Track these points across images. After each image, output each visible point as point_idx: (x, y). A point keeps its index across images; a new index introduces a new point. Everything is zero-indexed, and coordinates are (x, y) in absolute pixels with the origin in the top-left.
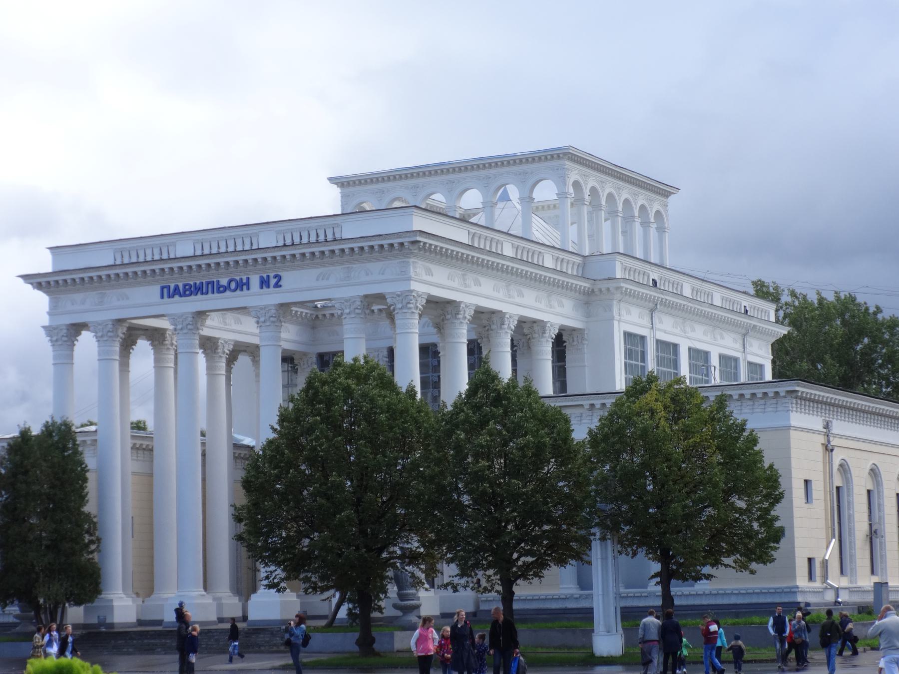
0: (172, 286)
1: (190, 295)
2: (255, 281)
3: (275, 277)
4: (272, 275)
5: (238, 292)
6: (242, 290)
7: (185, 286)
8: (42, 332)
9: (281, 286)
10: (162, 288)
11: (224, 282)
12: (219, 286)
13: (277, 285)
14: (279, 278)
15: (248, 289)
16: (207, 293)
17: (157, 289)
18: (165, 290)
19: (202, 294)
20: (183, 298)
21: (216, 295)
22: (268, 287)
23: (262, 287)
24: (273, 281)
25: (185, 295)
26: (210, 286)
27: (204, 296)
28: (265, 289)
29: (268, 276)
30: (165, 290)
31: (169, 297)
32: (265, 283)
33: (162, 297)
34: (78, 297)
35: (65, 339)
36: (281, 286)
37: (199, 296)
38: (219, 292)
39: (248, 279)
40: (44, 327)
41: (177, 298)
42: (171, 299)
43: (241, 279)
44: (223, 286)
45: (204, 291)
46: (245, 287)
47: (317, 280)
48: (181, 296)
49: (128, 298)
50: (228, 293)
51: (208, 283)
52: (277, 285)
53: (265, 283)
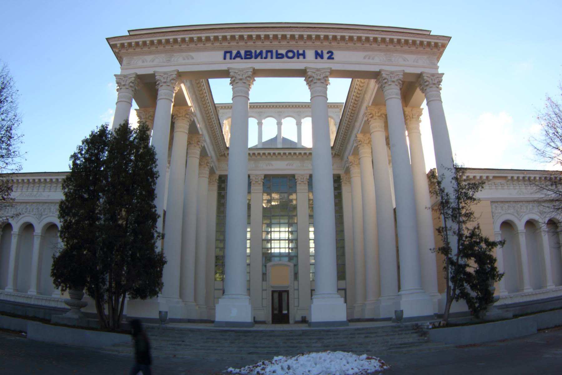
0: (234, 53)
1: (251, 58)
2: (310, 54)
3: (328, 53)
4: (325, 52)
5: (295, 59)
6: (298, 58)
7: (246, 52)
8: (114, 79)
9: (333, 59)
10: (226, 53)
11: (283, 52)
13: (330, 58)
15: (304, 58)
16: (266, 58)
17: (222, 53)
18: (228, 55)
19: (262, 58)
21: (274, 59)
23: (316, 58)
24: (326, 56)
25: (246, 58)
26: (269, 54)
27: (264, 60)
28: (319, 59)
29: (322, 52)
30: (228, 55)
31: (231, 59)
32: (319, 55)
33: (225, 58)
34: (149, 58)
35: (131, 84)
36: (333, 59)
37: (259, 59)
38: (277, 58)
39: (304, 51)
40: (115, 75)
41: (238, 59)
42: (232, 60)
43: (298, 51)
45: (264, 55)
46: (301, 57)
47: (365, 58)
48: (242, 59)
49: (193, 58)
50: (285, 59)
51: (267, 52)
52: (330, 58)
53: (319, 55)
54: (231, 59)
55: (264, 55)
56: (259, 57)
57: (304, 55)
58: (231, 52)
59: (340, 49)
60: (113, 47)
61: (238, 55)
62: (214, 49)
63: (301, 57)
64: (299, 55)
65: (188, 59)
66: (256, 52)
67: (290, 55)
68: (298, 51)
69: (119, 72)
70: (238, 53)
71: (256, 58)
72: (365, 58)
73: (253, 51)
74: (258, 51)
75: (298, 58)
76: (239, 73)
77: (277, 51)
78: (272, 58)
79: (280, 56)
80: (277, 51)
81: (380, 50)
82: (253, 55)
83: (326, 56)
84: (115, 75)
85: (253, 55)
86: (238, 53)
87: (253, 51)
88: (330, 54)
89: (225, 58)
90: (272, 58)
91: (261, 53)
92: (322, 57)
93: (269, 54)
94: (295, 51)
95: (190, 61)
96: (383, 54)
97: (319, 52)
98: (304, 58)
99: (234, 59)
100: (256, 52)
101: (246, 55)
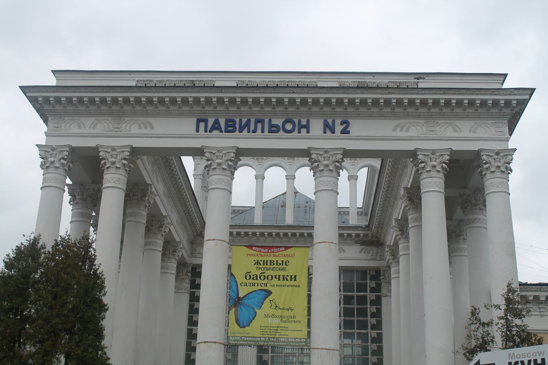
3: (341, 124)
6: (299, 132)
7: (227, 121)
8: (37, 151)
9: (348, 133)
10: (199, 121)
11: (278, 122)
12: (271, 126)
13: (345, 131)
14: (346, 123)
15: (308, 132)
16: (254, 131)
17: (194, 121)
18: (202, 125)
19: (249, 132)
20: (224, 133)
22: (333, 132)
23: (325, 133)
24: (339, 128)
26: (259, 126)
27: (251, 134)
30: (202, 125)
31: (206, 131)
33: (197, 131)
34: (88, 121)
36: (348, 133)
39: (308, 121)
40: (37, 145)
41: (216, 133)
42: (208, 133)
43: (300, 121)
44: (276, 126)
45: (252, 128)
46: (304, 131)
48: (221, 132)
49: (152, 127)
50: (281, 133)
53: (329, 127)
54: (206, 131)
55: (252, 128)
56: (246, 130)
57: (307, 127)
58: (206, 121)
59: (358, 116)
60: (33, 100)
61: (216, 126)
62: (181, 115)
63: (304, 131)
64: (301, 127)
65: (146, 128)
66: (241, 121)
67: (289, 127)
68: (300, 121)
69: (43, 141)
70: (217, 122)
71: (240, 131)
72: (395, 130)
73: (237, 120)
74: (244, 121)
75: (299, 132)
76: (218, 154)
77: (270, 121)
78: (263, 132)
79: (273, 129)
80: (270, 121)
81: (419, 117)
82: (237, 126)
83: (339, 128)
84: (37, 145)
85: (237, 126)
86: (217, 122)
87: (237, 120)
88: (345, 125)
89: (197, 131)
90: (263, 132)
91: (248, 124)
92: (333, 132)
93: (259, 126)
94: (296, 121)
95: (148, 131)
96: (422, 121)
97: (330, 121)
98: (308, 132)
99: (210, 131)
100: (241, 121)
101: (227, 126)
